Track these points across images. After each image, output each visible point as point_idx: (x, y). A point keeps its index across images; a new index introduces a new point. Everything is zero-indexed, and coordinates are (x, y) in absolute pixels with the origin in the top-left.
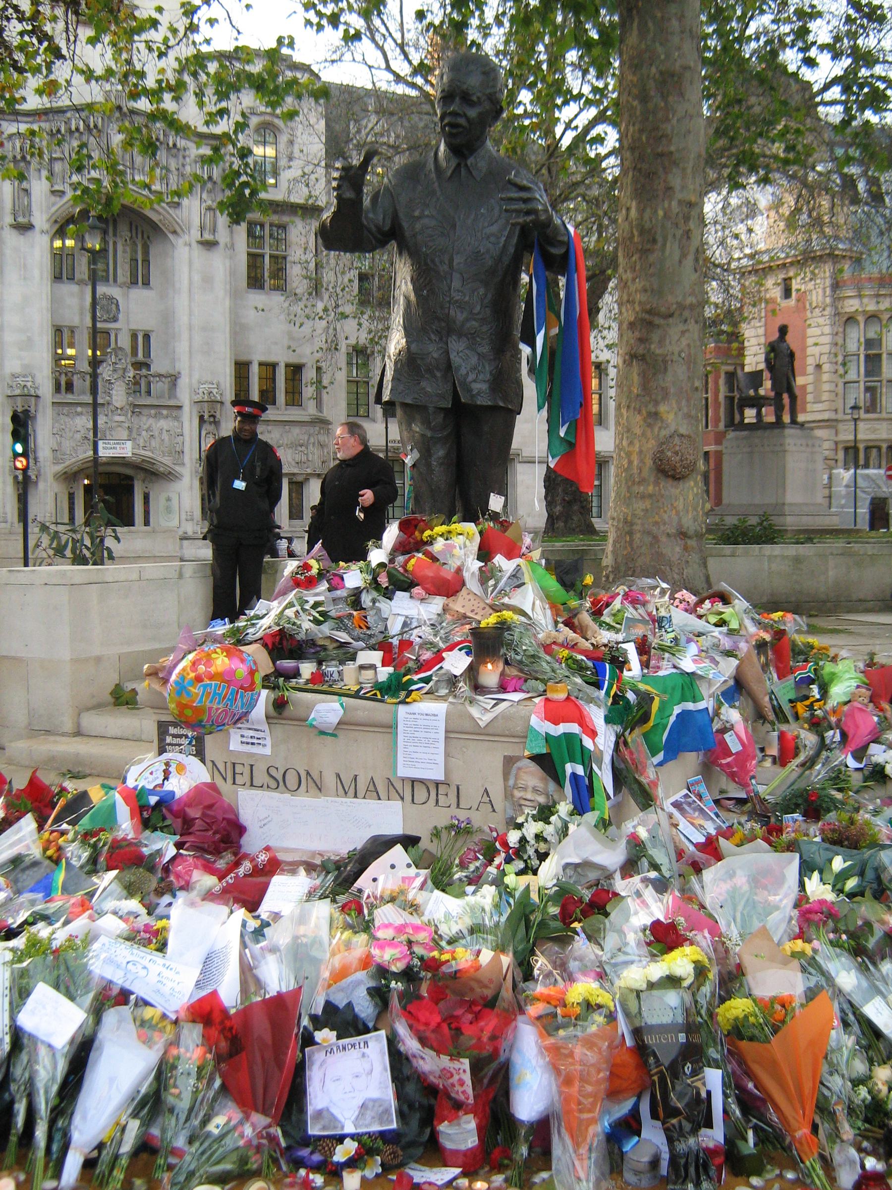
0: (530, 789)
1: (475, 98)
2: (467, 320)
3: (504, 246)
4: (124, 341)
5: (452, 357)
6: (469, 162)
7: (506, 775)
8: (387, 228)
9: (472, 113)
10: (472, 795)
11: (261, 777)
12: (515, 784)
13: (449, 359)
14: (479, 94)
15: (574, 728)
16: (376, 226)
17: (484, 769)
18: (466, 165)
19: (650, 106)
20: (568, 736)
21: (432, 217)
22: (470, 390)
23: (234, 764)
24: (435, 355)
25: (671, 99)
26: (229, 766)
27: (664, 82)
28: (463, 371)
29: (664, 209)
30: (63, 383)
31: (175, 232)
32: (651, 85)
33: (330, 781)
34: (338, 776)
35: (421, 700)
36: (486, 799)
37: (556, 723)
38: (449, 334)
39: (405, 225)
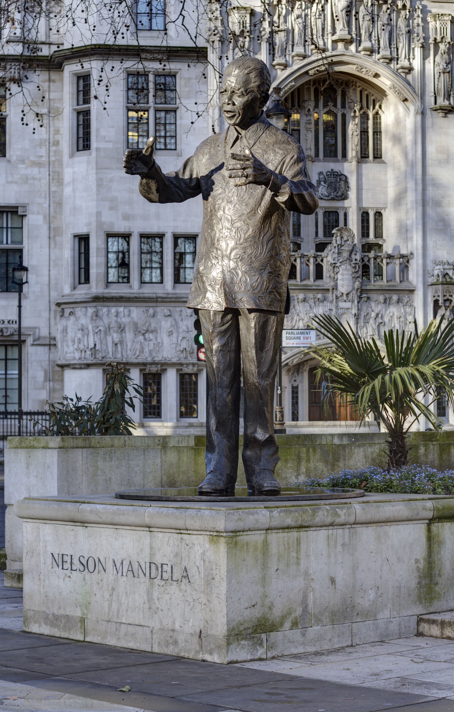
23: (63, 555)
26: (61, 556)
34: (114, 562)
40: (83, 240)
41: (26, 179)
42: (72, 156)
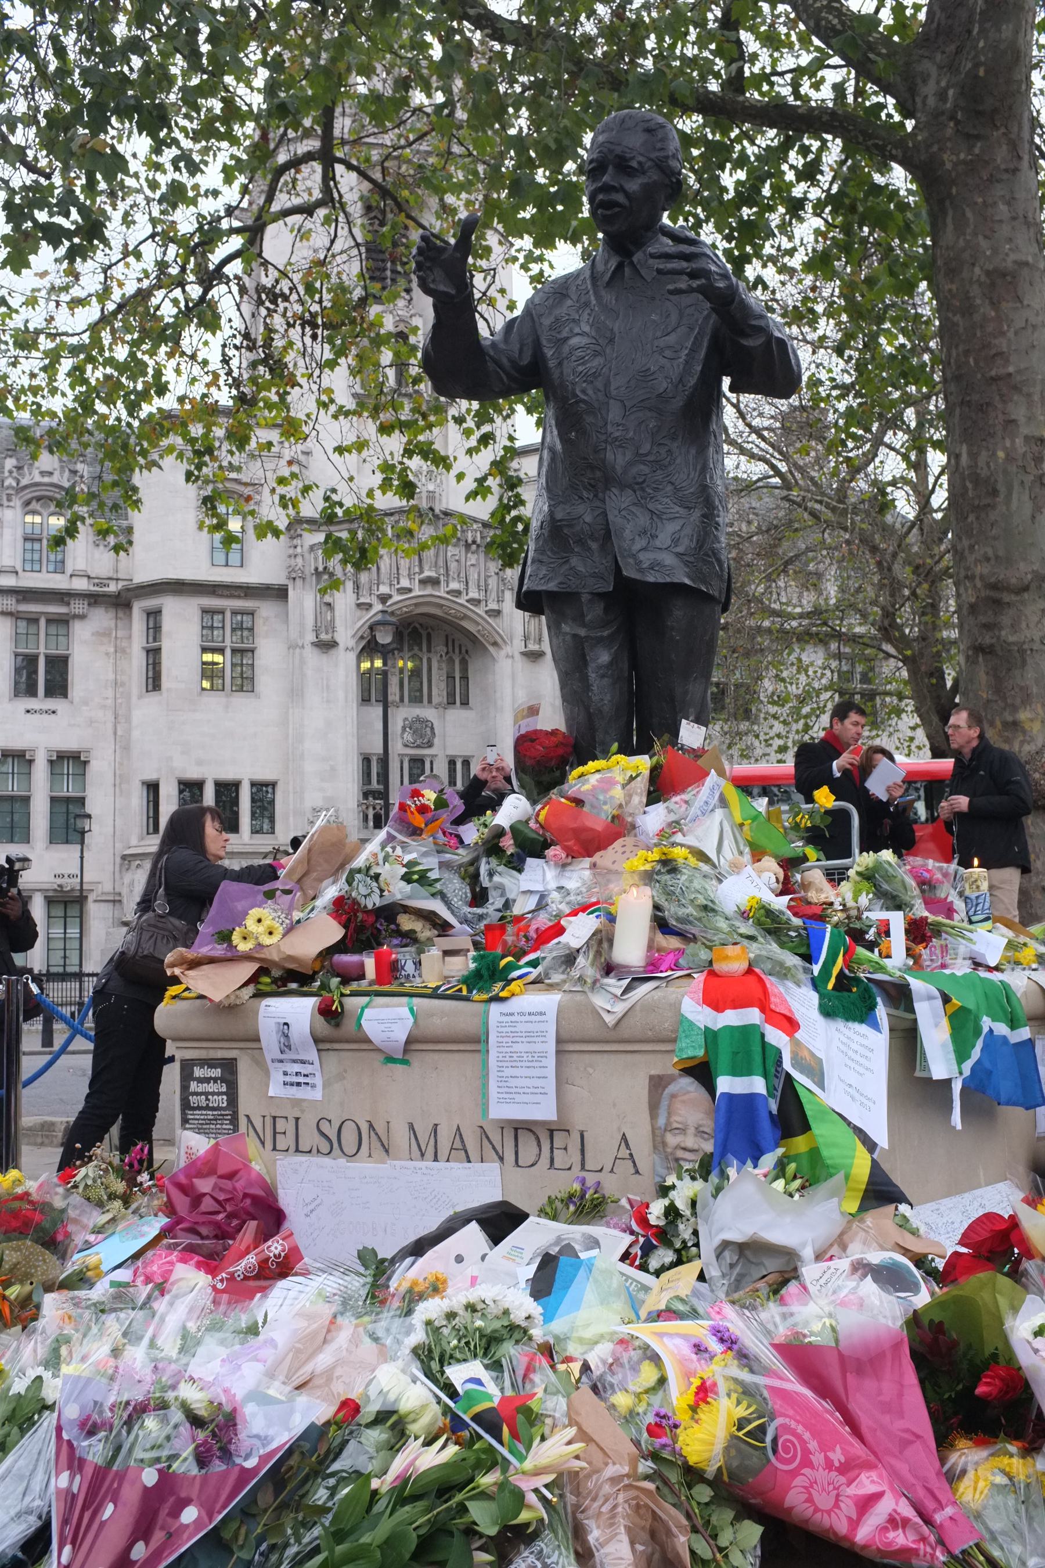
0: (691, 1131)
1: (634, 164)
2: (631, 464)
3: (687, 362)
4: (441, 769)
5: (611, 517)
6: (635, 259)
7: (654, 1108)
8: (525, 361)
9: (633, 186)
10: (603, 1149)
11: (309, 1138)
12: (668, 1123)
14: (641, 159)
15: (753, 1016)
16: (512, 361)
17: (616, 1102)
18: (632, 263)
19: (977, 317)
20: (746, 1032)
21: (583, 334)
24: (588, 518)
25: (1004, 305)
26: (269, 1121)
27: (993, 285)
28: (627, 534)
29: (1005, 449)
30: (371, 817)
31: (495, 644)
32: (975, 291)
33: (400, 1137)
34: (411, 1127)
35: (521, 993)
36: (624, 1152)
37: (718, 1008)
38: (607, 488)
40: (153, 788)
41: (91, 722)
42: (140, 697)
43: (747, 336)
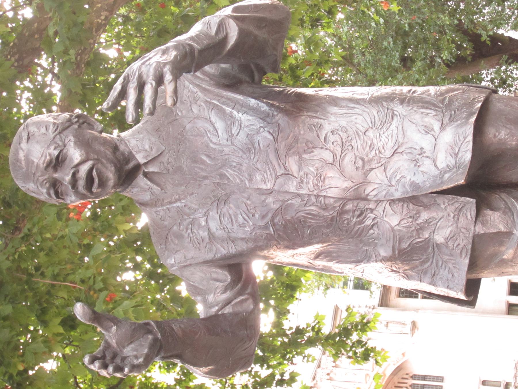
2: (342, 172)
6: (142, 161)
13: (399, 200)
18: (146, 164)
22: (449, 169)
39: (224, 250)
43: (225, 39)
